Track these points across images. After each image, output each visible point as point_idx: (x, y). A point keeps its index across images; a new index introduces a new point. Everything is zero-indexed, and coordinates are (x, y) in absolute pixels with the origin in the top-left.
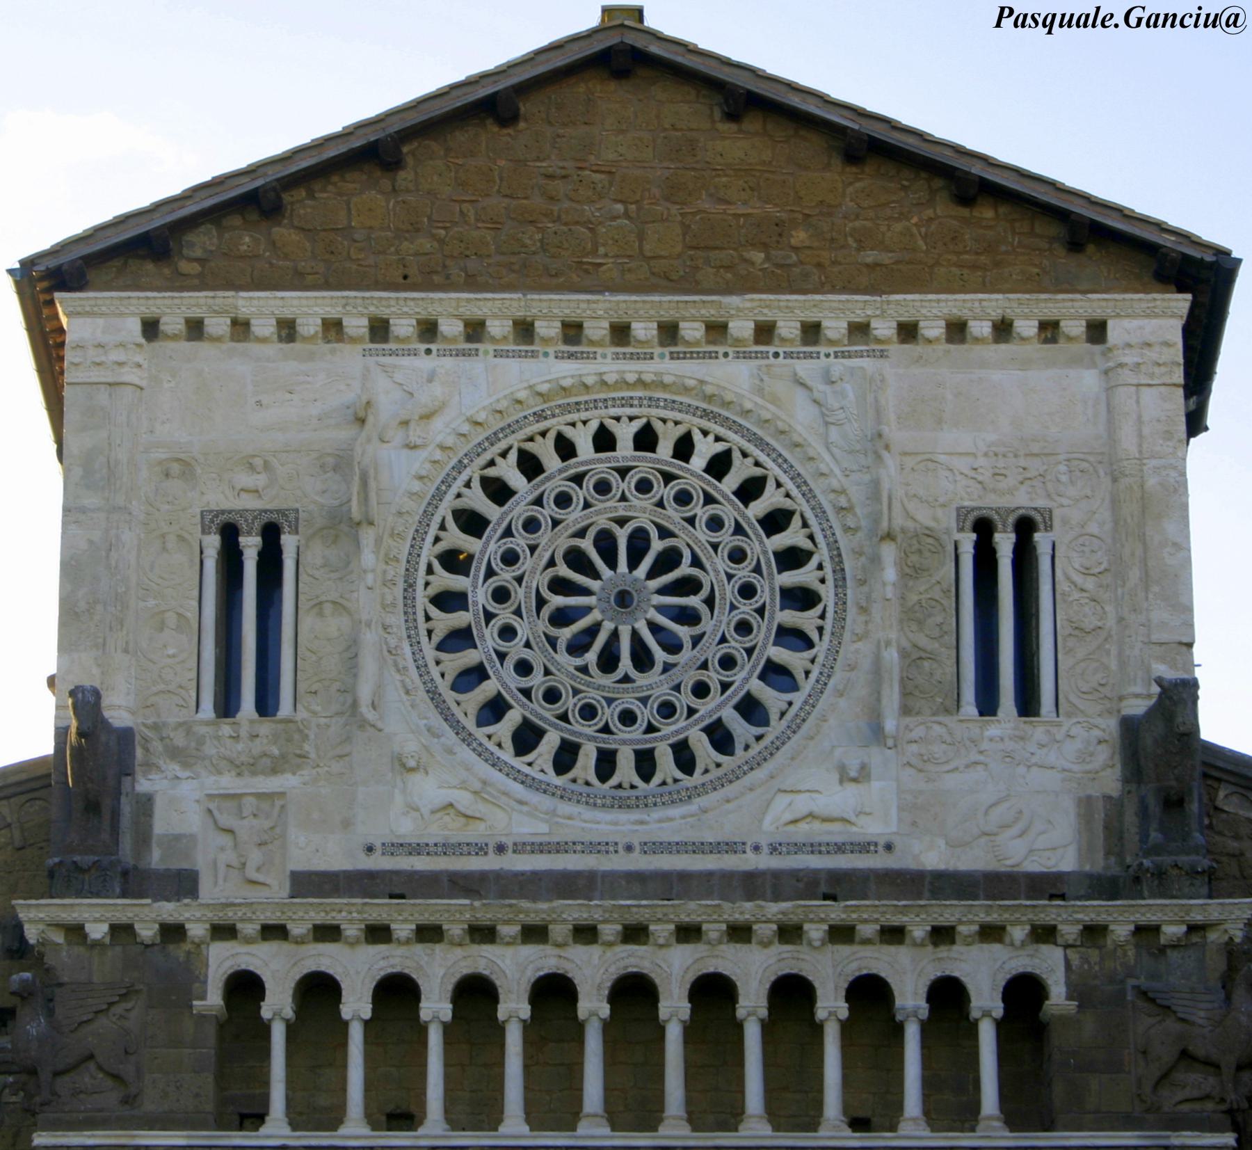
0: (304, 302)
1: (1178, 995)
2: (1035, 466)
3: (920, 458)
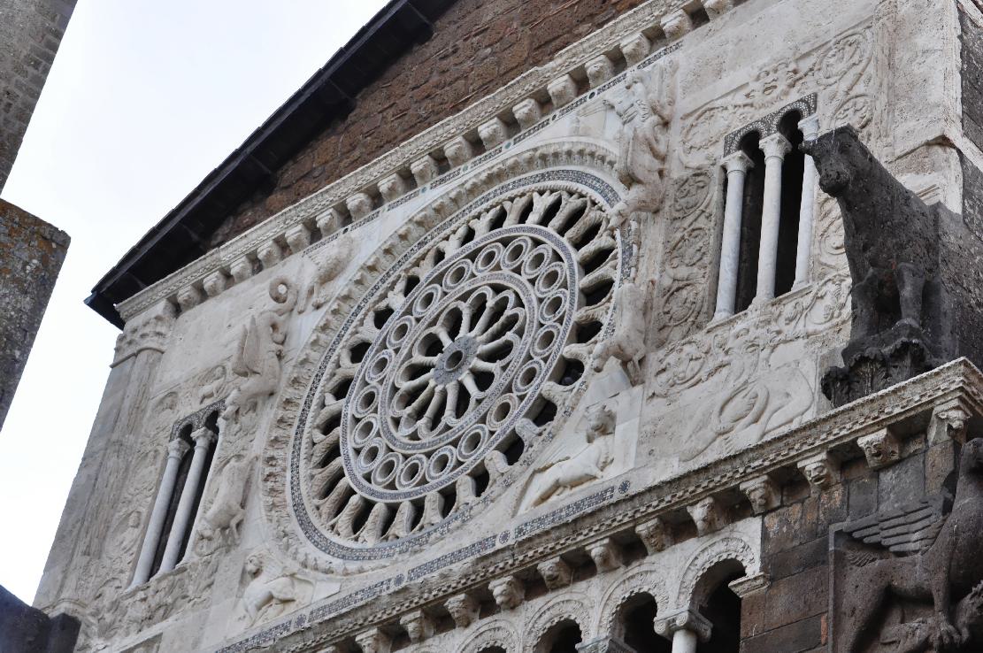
0: (259, 232)
1: (887, 524)
2: (804, 66)
3: (696, 115)
